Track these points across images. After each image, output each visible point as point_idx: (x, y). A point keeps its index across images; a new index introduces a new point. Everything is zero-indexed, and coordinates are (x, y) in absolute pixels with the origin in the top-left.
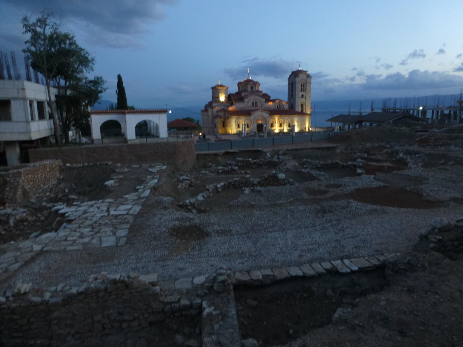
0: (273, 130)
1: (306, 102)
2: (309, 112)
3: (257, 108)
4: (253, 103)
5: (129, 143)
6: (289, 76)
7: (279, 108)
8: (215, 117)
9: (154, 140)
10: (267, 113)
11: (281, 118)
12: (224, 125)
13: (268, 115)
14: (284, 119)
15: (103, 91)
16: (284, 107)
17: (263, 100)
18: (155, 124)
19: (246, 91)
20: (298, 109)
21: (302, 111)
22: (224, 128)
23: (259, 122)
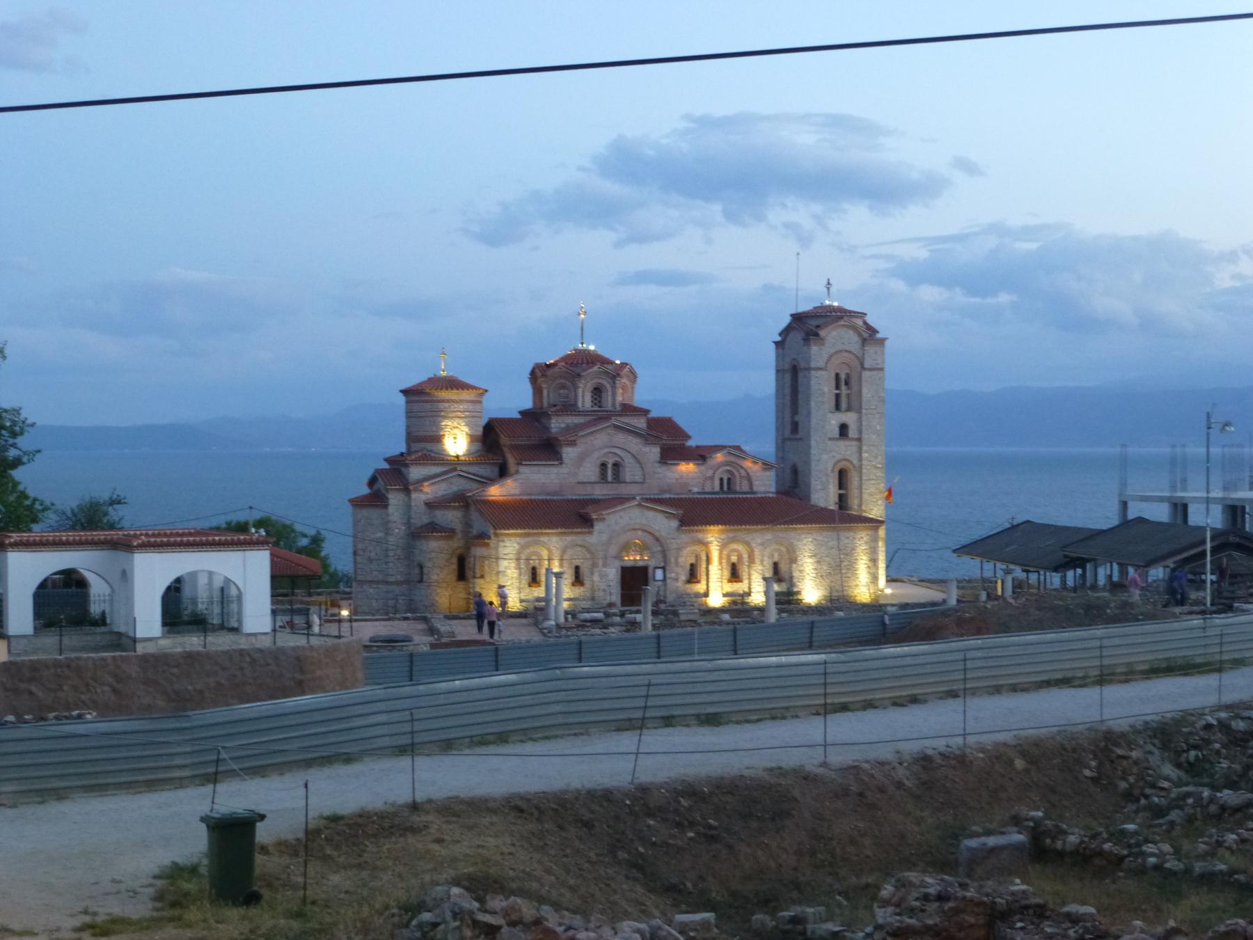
0: (698, 595)
1: (860, 459)
2: (876, 509)
3: (624, 490)
4: (604, 465)
5: (140, 649)
7: (729, 488)
8: (417, 533)
9: (220, 642)
11: (733, 540)
12: (463, 570)
13: (674, 524)
14: (748, 544)
15: (25, 459)
16: (751, 484)
17: (654, 452)
18: (218, 583)
19: (569, 408)
20: (824, 494)
21: (843, 501)
22: (461, 584)
23: (633, 558)
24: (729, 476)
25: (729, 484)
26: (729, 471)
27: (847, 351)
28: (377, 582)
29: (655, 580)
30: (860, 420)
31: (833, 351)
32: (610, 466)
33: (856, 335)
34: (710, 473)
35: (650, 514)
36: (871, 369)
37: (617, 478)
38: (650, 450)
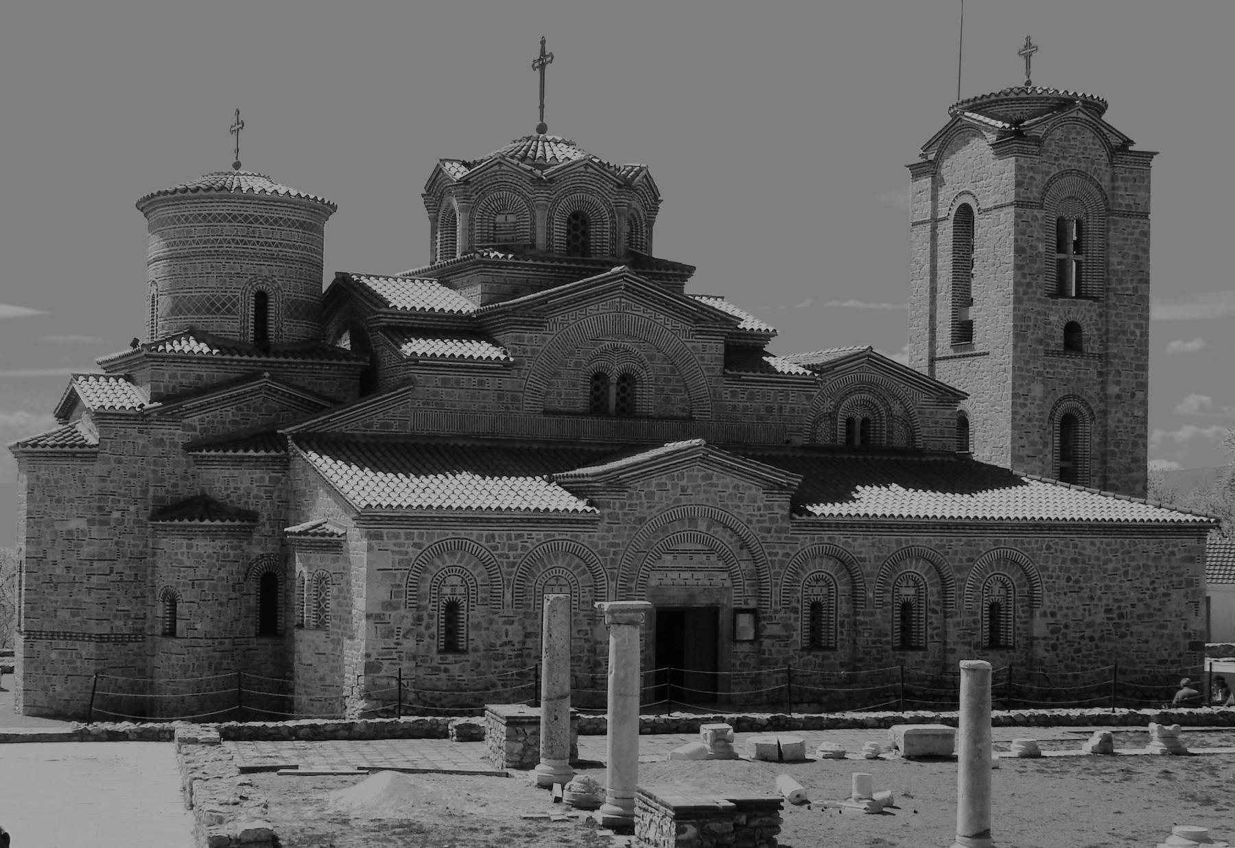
4: (599, 379)
6: (927, 147)
7: (862, 442)
10: (773, 488)
16: (912, 434)
24: (868, 414)
25: (863, 432)
26: (867, 404)
27: (1080, 173)
28: (67, 636)
29: (734, 639)
30: (1100, 315)
31: (1055, 171)
32: (614, 379)
33: (1097, 141)
34: (828, 406)
35: (728, 480)
36: (1123, 215)
37: (627, 408)
38: (704, 347)
